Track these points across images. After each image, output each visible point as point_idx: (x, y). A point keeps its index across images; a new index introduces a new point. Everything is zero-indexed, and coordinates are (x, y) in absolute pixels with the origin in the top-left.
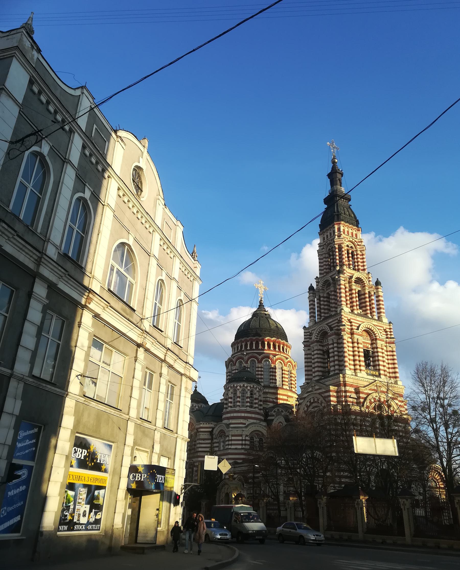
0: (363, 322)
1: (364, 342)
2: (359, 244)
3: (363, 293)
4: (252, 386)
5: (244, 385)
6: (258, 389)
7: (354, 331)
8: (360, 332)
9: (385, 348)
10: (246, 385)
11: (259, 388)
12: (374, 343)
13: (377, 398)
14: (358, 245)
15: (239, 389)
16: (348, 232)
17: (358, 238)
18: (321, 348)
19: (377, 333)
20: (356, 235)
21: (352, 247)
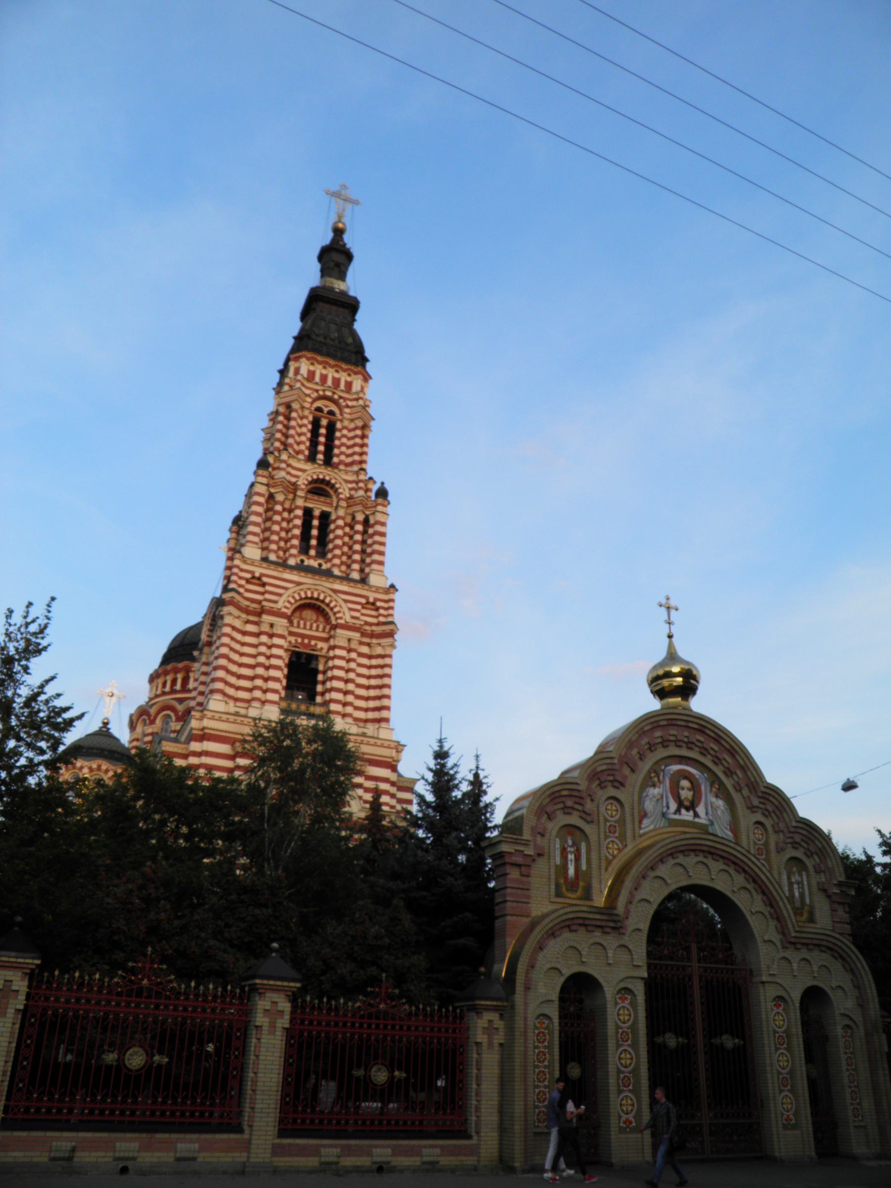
0: (299, 584)
1: (291, 634)
2: (350, 403)
8: (286, 607)
9: (365, 650)
12: (331, 637)
14: (347, 406)
16: (324, 378)
19: (339, 612)
20: (349, 385)
21: (331, 413)
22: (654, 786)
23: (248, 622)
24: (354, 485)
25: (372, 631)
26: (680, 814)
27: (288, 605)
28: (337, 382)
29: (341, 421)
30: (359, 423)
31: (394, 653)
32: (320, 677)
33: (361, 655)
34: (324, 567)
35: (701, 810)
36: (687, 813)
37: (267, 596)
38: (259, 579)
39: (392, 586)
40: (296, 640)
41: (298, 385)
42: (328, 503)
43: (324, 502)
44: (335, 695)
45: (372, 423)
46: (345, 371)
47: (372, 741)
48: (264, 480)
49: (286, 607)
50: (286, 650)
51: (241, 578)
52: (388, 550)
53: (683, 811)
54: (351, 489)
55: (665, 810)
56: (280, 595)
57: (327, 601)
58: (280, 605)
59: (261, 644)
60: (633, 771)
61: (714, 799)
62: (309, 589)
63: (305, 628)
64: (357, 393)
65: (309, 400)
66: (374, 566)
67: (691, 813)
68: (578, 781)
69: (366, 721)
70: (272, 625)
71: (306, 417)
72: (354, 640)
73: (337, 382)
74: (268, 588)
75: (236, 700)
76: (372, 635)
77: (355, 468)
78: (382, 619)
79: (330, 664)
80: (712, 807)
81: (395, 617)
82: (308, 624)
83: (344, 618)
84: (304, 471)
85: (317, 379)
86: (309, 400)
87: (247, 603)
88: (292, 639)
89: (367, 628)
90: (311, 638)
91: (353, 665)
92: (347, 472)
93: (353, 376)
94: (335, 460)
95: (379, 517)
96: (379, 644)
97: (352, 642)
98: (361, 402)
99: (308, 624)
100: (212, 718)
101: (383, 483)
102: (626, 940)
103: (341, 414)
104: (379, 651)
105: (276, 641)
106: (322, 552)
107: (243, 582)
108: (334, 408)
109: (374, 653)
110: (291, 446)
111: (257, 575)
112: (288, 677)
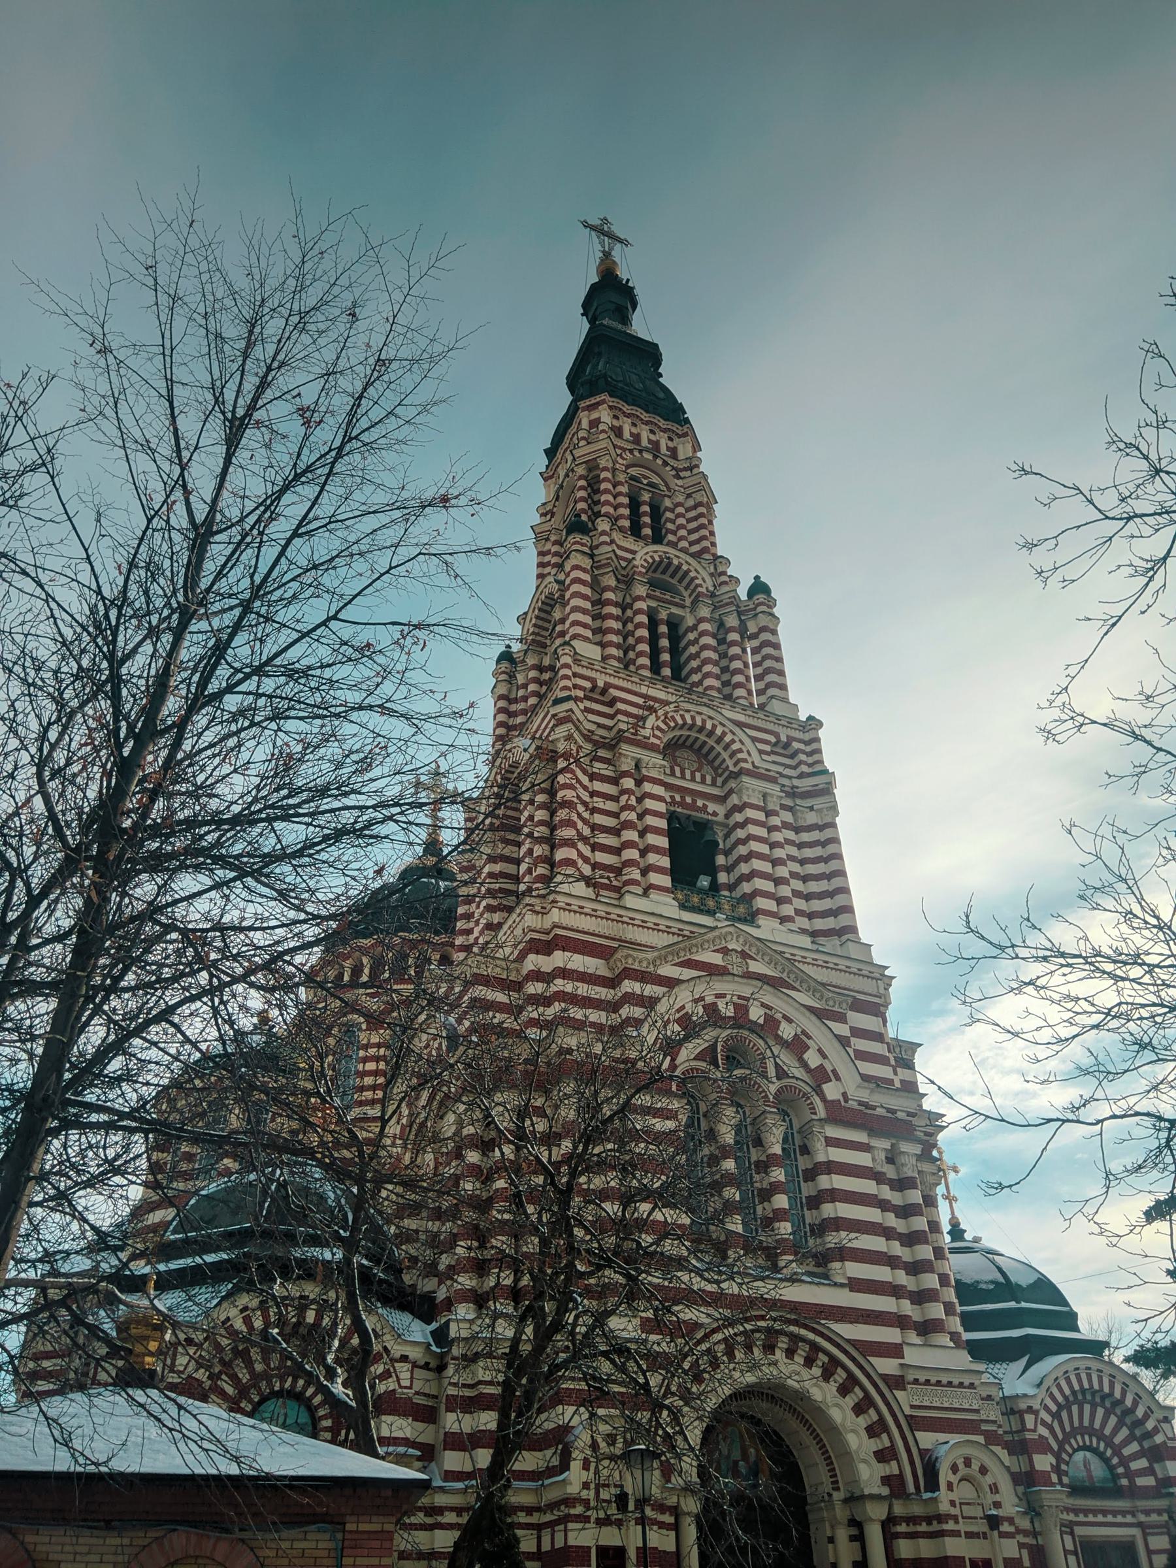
3: (690, 621)
12: (731, 791)
17: (681, 456)
18: (508, 851)
21: (651, 484)
25: (793, 787)
32: (720, 860)
46: (665, 431)
72: (772, 796)
76: (793, 793)
78: (804, 768)
79: (741, 833)
83: (750, 760)
87: (593, 727)
96: (811, 808)
97: (769, 798)
100: (567, 908)
104: (811, 818)
109: (801, 823)
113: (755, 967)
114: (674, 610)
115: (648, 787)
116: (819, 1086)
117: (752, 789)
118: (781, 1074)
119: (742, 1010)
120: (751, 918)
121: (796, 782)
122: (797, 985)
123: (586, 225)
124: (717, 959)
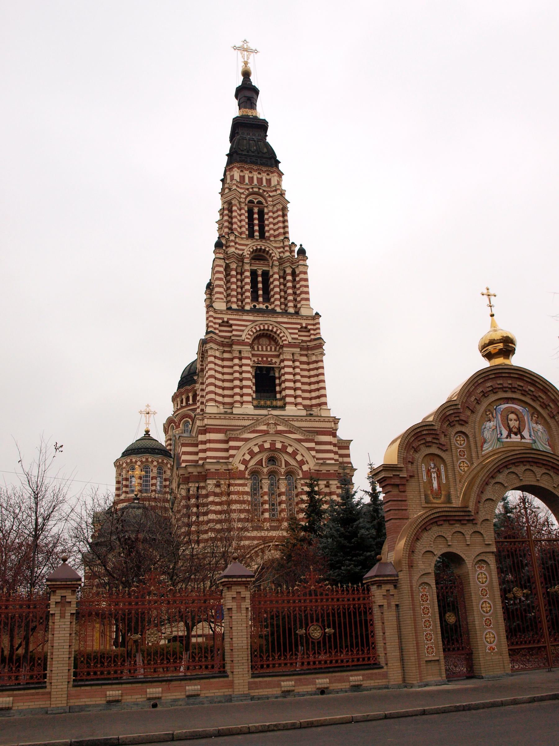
0: (254, 321)
2: (271, 194)
4: (144, 460)
5: (131, 460)
6: (155, 463)
7: (232, 340)
8: (247, 338)
9: (304, 359)
10: (134, 460)
11: (158, 462)
12: (280, 354)
13: (267, 446)
14: (270, 196)
15: (125, 468)
16: (251, 179)
17: (273, 184)
19: (284, 336)
20: (269, 181)
21: (260, 203)
22: (490, 420)
23: (224, 352)
24: (282, 250)
26: (511, 438)
27: (249, 337)
28: (260, 180)
29: (267, 207)
30: (280, 207)
31: (324, 358)
32: (277, 381)
33: (302, 363)
34: (270, 308)
35: (525, 433)
36: (516, 437)
37: (234, 333)
38: (227, 322)
39: (317, 314)
40: (258, 359)
41: (234, 187)
42: (266, 265)
43: (263, 264)
44: (288, 392)
45: (288, 205)
47: (317, 419)
48: (221, 256)
49: (247, 338)
50: (252, 367)
51: (215, 323)
52: (311, 290)
53: (513, 436)
54: (280, 253)
55: (499, 436)
56: (243, 331)
57: (275, 330)
58: (244, 337)
59: (235, 365)
60: (473, 412)
61: (534, 425)
62: (261, 324)
63: (262, 350)
64: (275, 186)
65: (243, 196)
66: (303, 302)
67: (519, 436)
68: (434, 424)
69: (312, 406)
70: (240, 352)
71: (243, 208)
73: (260, 180)
74: (234, 327)
75: (224, 404)
76: (308, 349)
77: (281, 238)
78: (312, 337)
80: (533, 431)
81: (321, 334)
82: (264, 347)
84: (247, 245)
85: (247, 181)
86: (243, 196)
87: (222, 340)
88: (255, 359)
89: (304, 344)
90: (267, 356)
91: (298, 370)
92: (276, 241)
93: (271, 175)
94: (267, 234)
95: (301, 269)
96: (313, 354)
98: (279, 192)
99: (264, 347)
100: (210, 418)
101: (301, 245)
102: (478, 528)
103: (267, 203)
104: (314, 358)
105: (244, 361)
106: (267, 298)
107: (217, 326)
108: (261, 199)
109: (310, 361)
110: (236, 229)
111: (225, 320)
112: (256, 384)
113: (280, 428)
114: (264, 269)
115: (244, 361)
116: (301, 467)
117: (287, 353)
118: (287, 463)
119: (273, 444)
120: (283, 407)
121: (308, 344)
122: (296, 432)
123: (235, 48)
124: (264, 428)
